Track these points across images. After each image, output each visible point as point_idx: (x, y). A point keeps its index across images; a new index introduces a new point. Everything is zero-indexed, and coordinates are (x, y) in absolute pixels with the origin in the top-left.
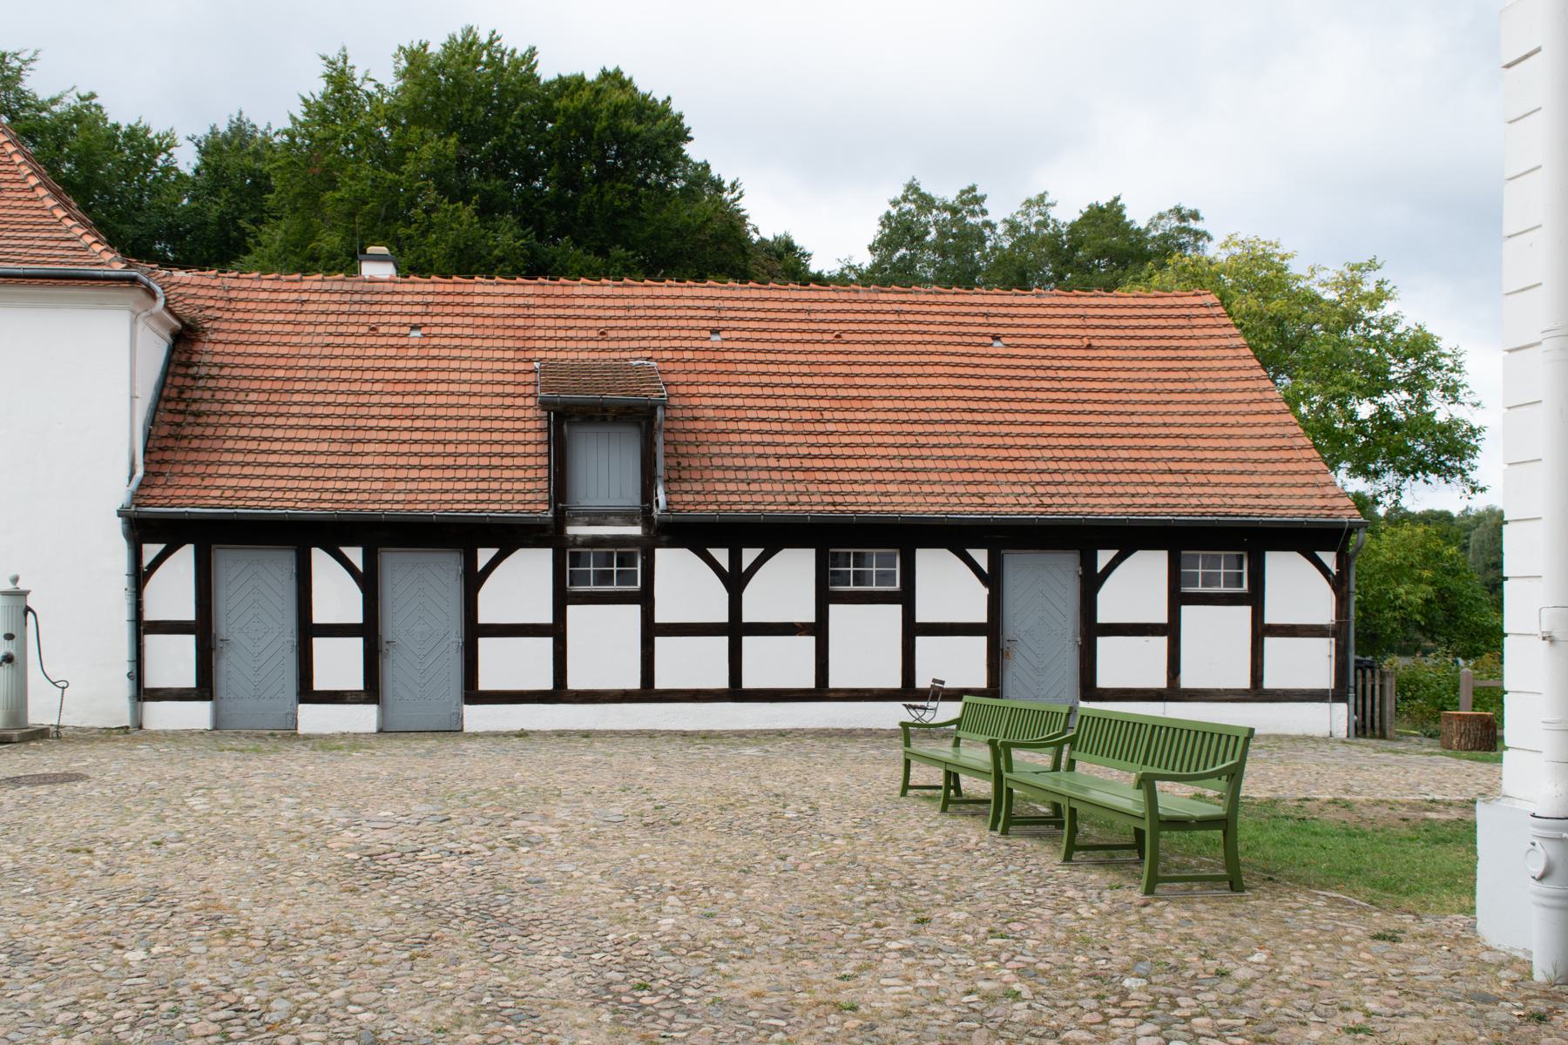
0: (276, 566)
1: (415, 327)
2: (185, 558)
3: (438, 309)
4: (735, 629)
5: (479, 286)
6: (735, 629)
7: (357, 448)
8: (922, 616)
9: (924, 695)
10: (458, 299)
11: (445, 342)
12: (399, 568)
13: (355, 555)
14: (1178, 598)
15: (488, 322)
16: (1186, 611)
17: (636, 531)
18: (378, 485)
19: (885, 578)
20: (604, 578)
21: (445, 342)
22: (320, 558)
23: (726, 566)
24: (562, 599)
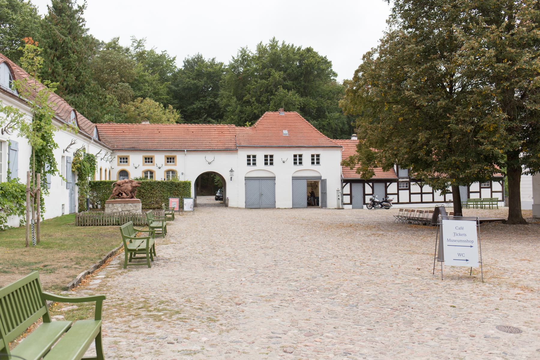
0: (360, 186)
2: (348, 185)
4: (422, 193)
6: (422, 193)
12: (377, 186)
13: (371, 184)
14: (481, 188)
16: (482, 189)
17: (408, 180)
20: (403, 187)
22: (366, 184)
24: (398, 190)
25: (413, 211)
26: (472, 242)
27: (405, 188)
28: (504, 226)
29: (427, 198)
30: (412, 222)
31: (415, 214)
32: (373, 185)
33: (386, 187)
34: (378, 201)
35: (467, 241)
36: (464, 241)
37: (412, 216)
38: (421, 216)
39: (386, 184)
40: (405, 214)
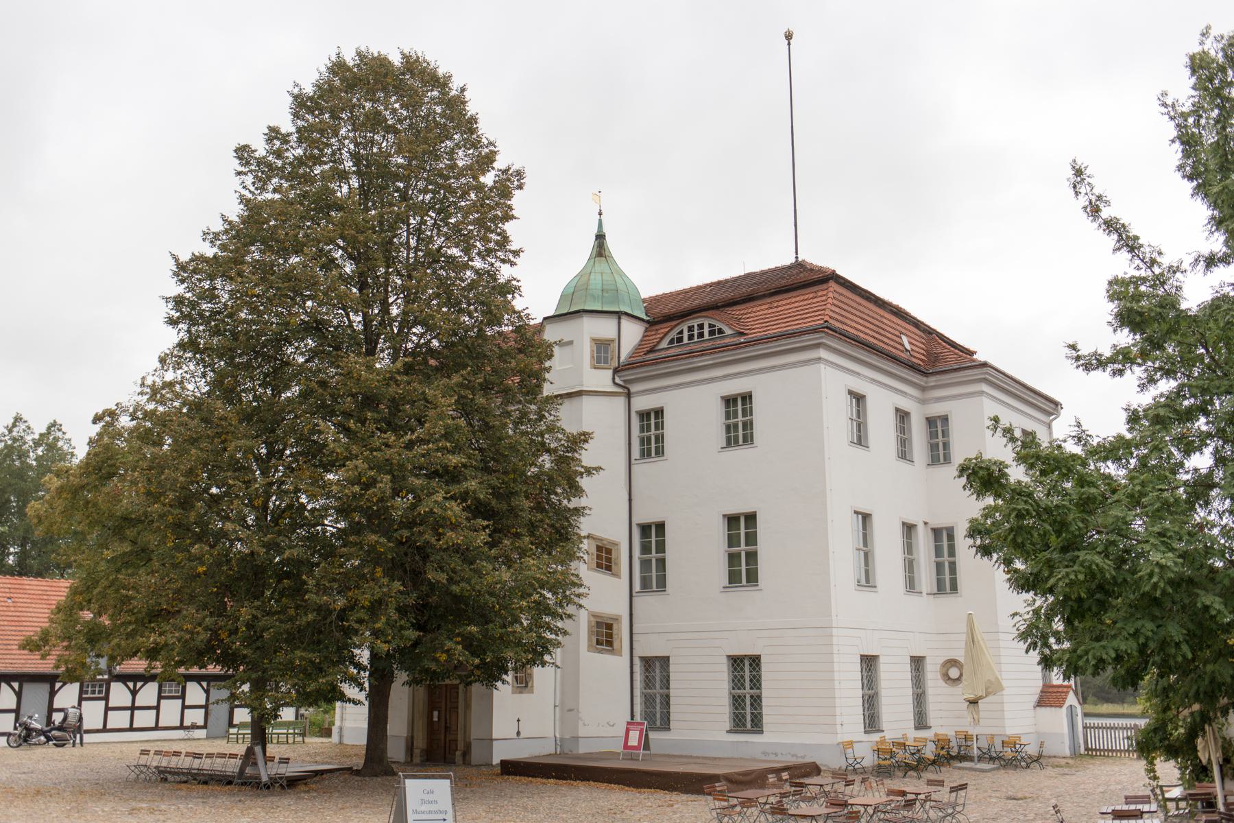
1: (8, 598)
3: (14, 591)
5: (25, 581)
6: (133, 708)
7: (9, 647)
8: (187, 703)
9: (187, 728)
10: (20, 587)
11: (22, 605)
13: (16, 685)
15: (34, 597)
17: (106, 677)
18: (23, 661)
19: (177, 691)
20: (93, 692)
21: (22, 605)
23: (132, 687)
25: (177, 754)
26: (445, 812)
27: (96, 695)
28: (361, 781)
29: (144, 718)
30: (169, 777)
31: (150, 759)
32: (21, 687)
33: (53, 694)
34: (39, 727)
35: (439, 812)
36: (436, 812)
37: (173, 765)
38: (197, 763)
39: (52, 687)
40: (154, 761)
